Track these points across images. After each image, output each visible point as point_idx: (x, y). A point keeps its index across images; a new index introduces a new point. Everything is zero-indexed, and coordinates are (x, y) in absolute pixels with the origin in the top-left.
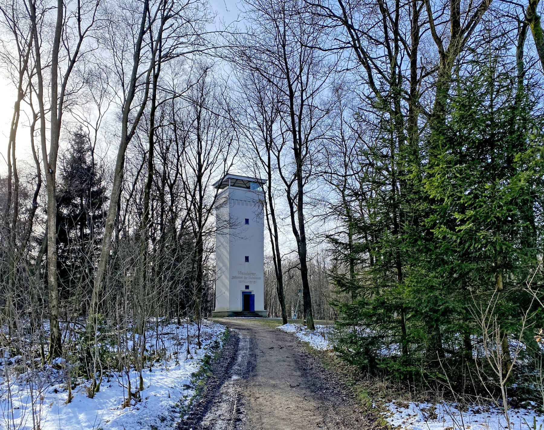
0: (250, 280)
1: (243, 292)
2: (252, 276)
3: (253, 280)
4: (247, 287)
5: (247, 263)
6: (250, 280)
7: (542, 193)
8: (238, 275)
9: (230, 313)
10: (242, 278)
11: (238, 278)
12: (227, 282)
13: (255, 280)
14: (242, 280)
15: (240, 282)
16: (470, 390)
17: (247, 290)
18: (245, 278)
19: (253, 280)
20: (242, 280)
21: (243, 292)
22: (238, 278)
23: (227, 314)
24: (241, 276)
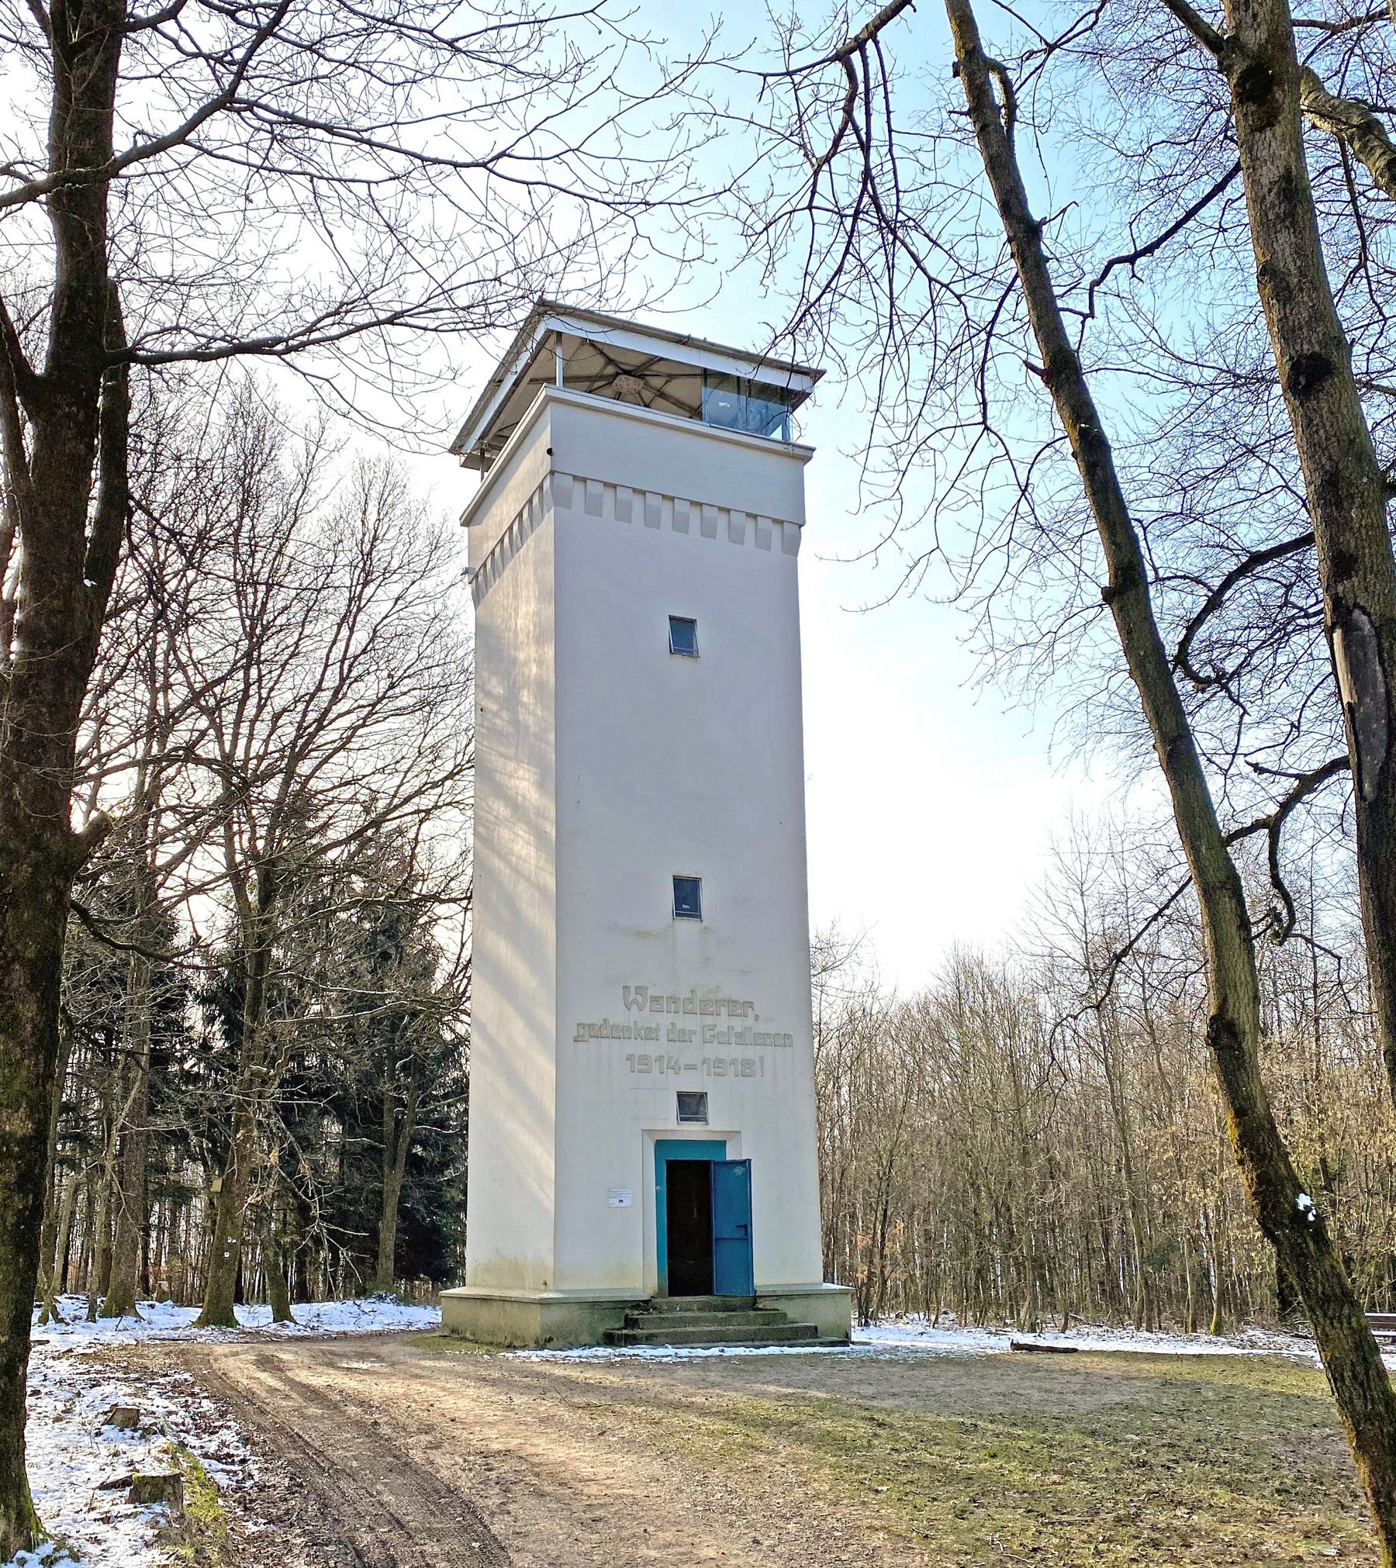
0: (713, 1051)
1: (660, 1145)
2: (723, 1022)
3: (736, 1052)
4: (691, 1105)
5: (686, 926)
6: (713, 1051)
7: (1390, 110)
8: (619, 1016)
9: (556, 1315)
10: (650, 1034)
11: (620, 1033)
12: (541, 1071)
13: (751, 1052)
14: (652, 1049)
15: (641, 1064)
16: (1310, 422)
17: (692, 1131)
18: (680, 1037)
19: (736, 1052)
20: (652, 1049)
21: (660, 1145)
22: (620, 1033)
23: (534, 1322)
24: (646, 1017)
